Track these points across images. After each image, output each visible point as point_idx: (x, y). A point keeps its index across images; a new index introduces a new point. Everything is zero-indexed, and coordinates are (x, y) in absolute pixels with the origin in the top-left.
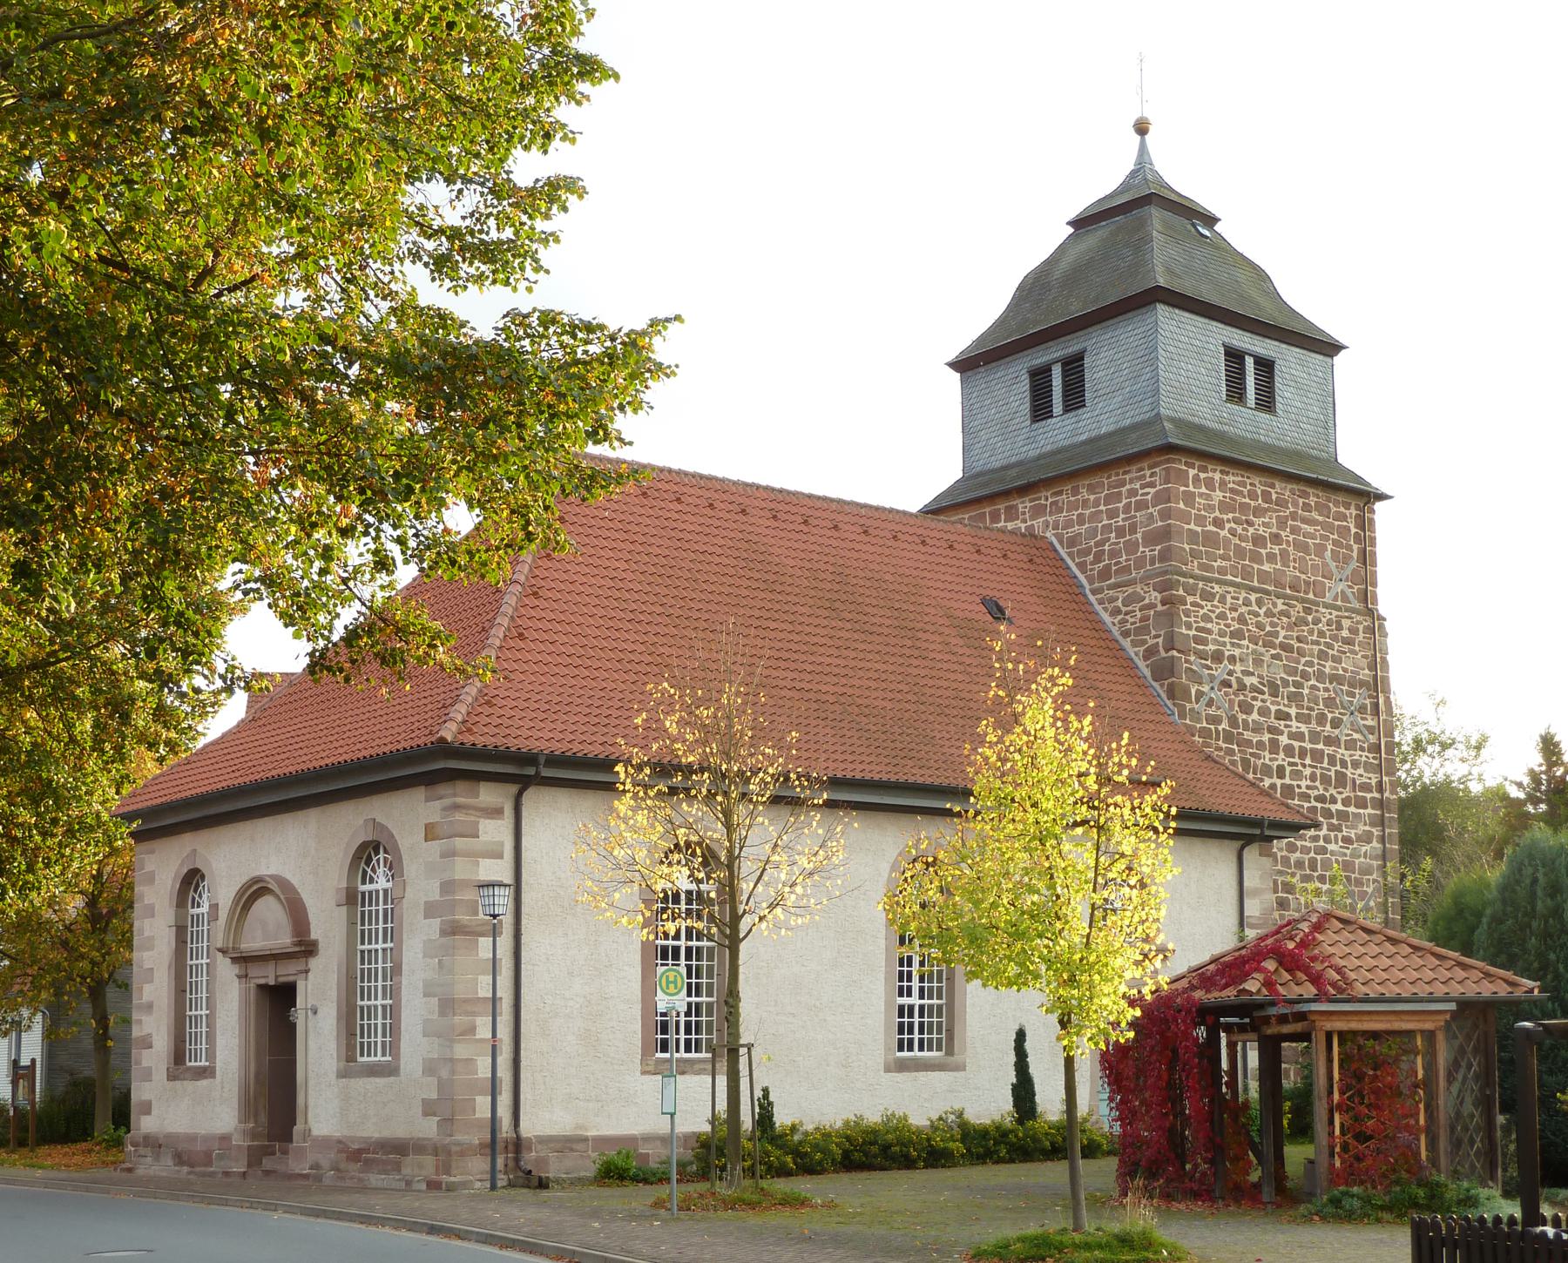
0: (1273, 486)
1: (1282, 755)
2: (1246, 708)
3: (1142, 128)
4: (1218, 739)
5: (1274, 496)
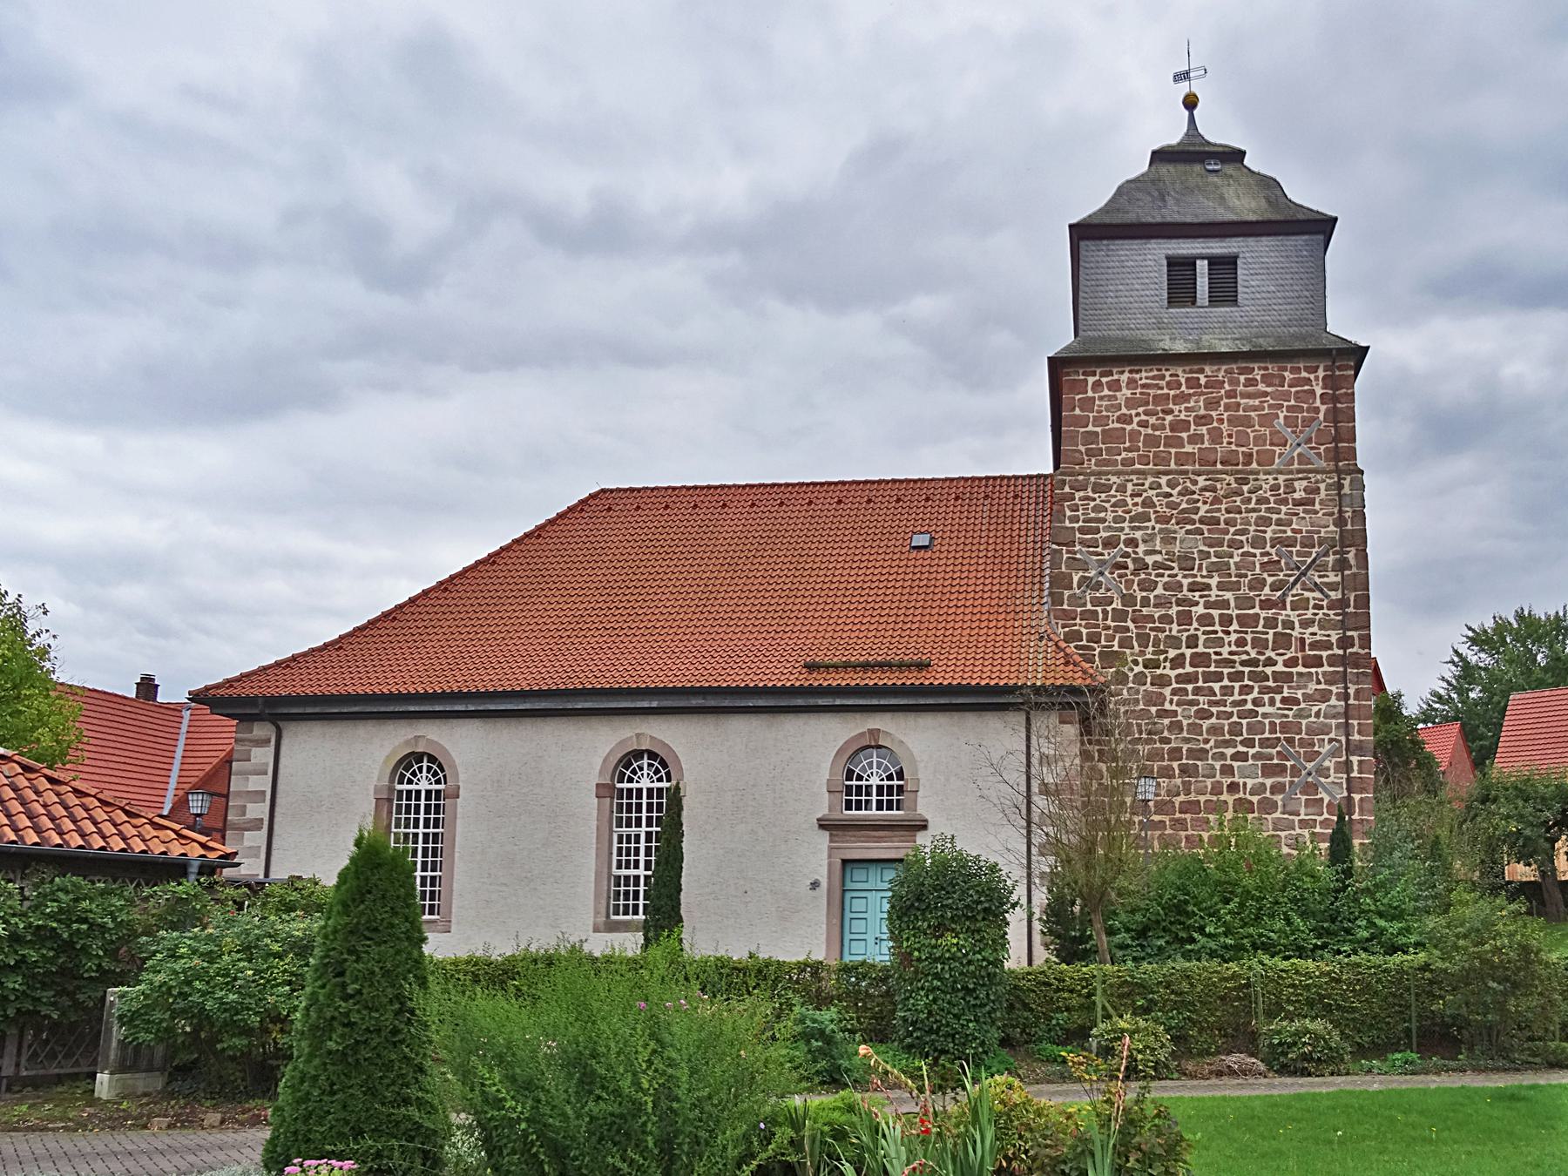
0: (1202, 371)
1: (1195, 625)
2: (1148, 586)
3: (1190, 103)
4: (1105, 619)
5: (1203, 381)
